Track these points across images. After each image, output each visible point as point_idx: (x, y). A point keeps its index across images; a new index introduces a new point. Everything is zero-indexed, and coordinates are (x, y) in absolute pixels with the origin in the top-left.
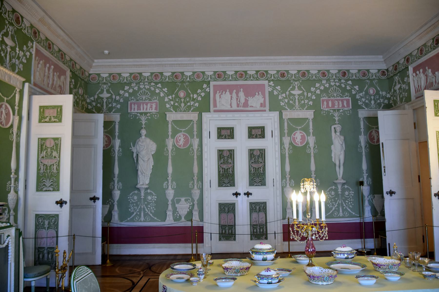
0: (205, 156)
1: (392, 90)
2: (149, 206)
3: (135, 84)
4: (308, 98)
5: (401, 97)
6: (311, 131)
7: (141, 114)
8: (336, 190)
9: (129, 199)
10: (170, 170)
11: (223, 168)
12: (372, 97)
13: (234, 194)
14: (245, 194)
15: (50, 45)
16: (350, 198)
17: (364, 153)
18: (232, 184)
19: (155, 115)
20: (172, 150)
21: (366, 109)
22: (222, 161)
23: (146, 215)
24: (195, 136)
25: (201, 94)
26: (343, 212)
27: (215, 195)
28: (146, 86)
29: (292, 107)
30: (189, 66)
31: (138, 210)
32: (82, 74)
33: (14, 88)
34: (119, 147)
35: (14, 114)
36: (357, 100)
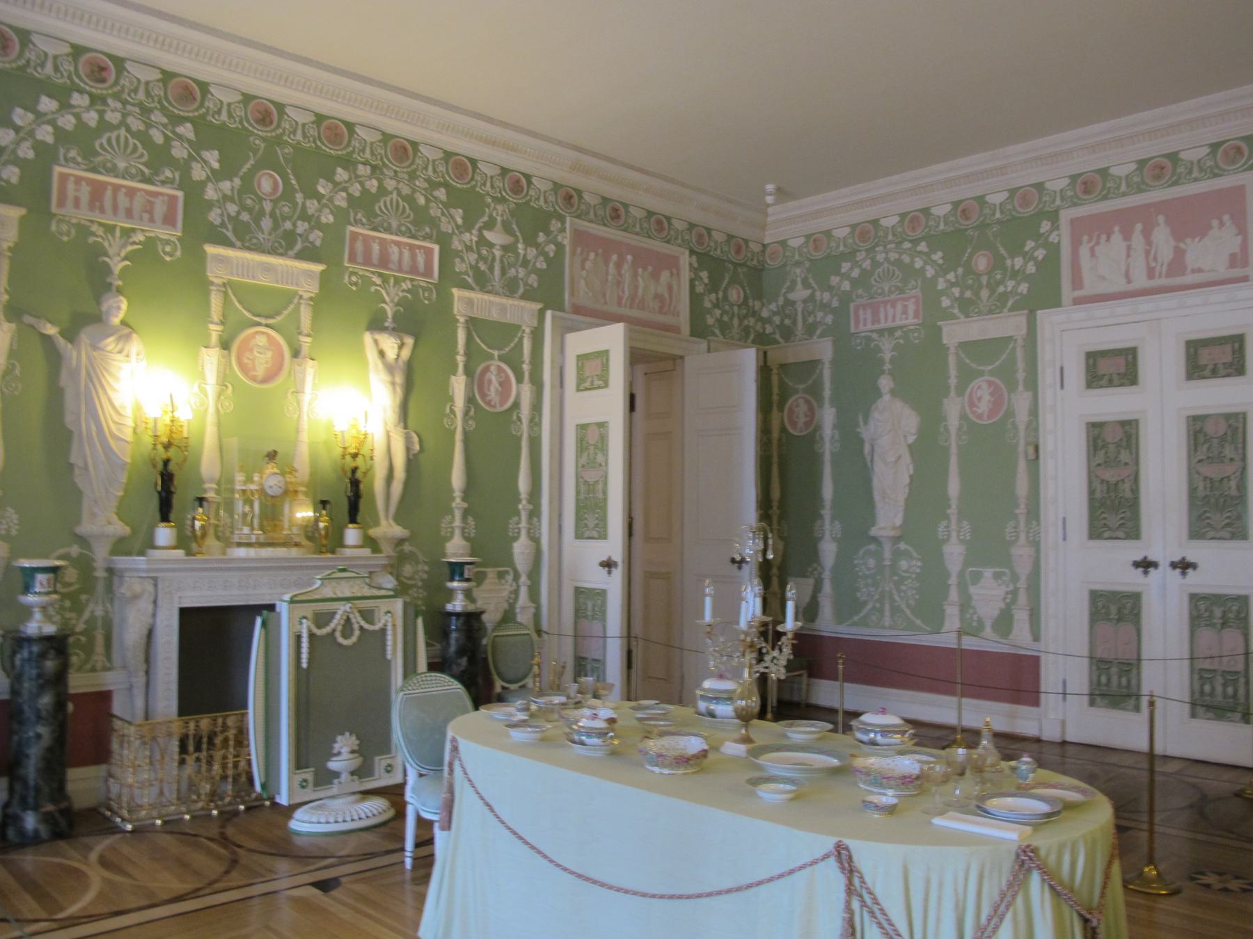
0: (1048, 444)
2: (903, 588)
7: (880, 332)
10: (954, 487)
11: (1102, 481)
13: (1137, 564)
14: (1174, 565)
15: (616, 210)
18: (1130, 529)
20: (960, 429)
22: (1100, 457)
24: (1021, 383)
25: (1036, 254)
27: (1076, 566)
30: (992, 175)
32: (738, 252)
33: (519, 327)
34: (835, 427)
35: (520, 380)
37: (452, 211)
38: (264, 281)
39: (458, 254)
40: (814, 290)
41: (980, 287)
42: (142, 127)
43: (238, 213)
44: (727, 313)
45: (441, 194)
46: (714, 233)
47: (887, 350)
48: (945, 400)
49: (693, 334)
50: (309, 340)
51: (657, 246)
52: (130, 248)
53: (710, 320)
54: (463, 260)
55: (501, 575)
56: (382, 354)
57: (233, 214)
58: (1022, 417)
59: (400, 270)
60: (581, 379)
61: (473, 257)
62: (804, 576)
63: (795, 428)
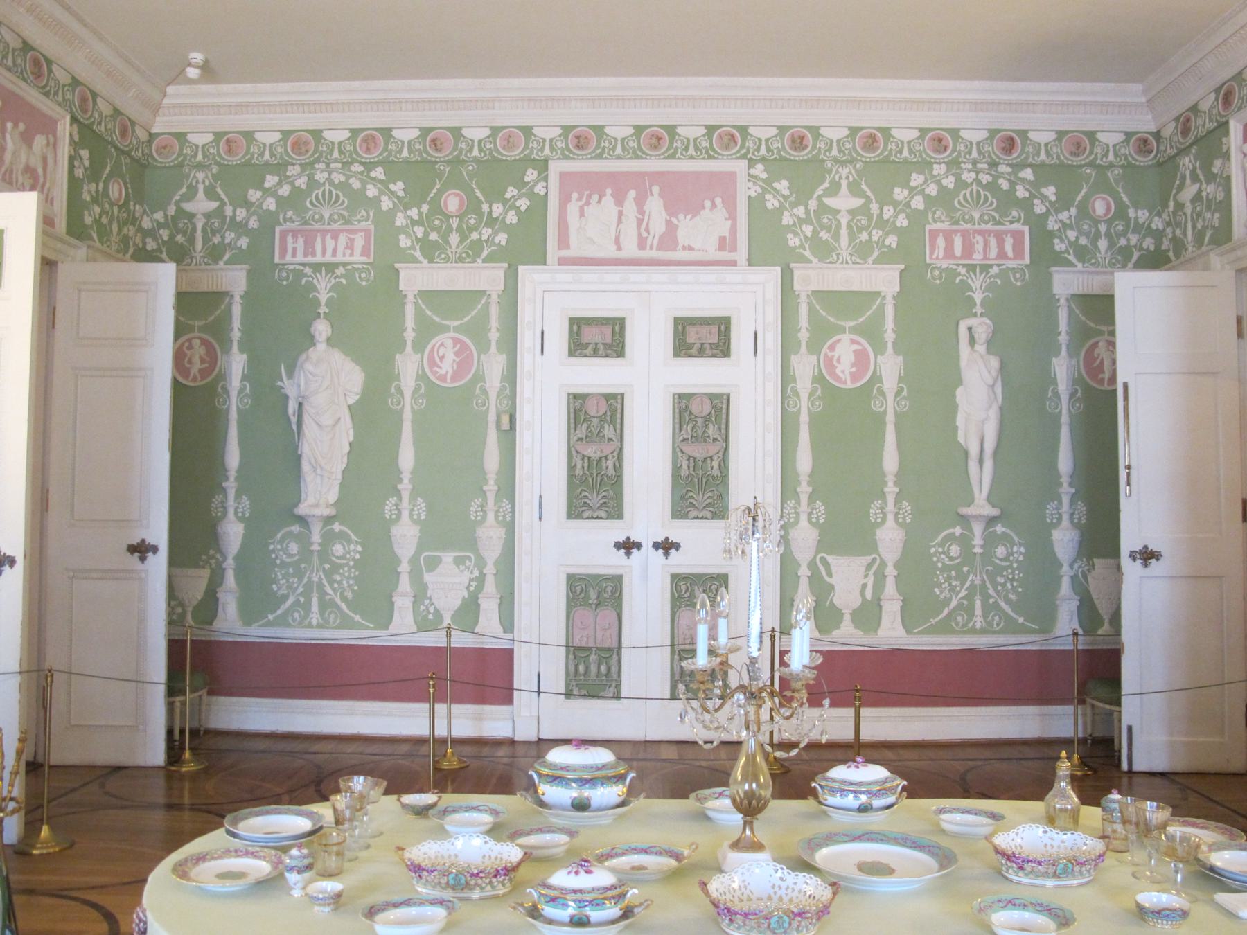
0: (524, 414)
1: (1172, 204)
2: (338, 577)
3: (298, 169)
4: (882, 223)
5: (1199, 226)
6: (890, 336)
7: (317, 267)
8: (965, 541)
9: (273, 551)
10: (407, 458)
11: (584, 456)
12: (1103, 228)
13: (618, 546)
14: (656, 546)
16: (1011, 567)
17: (1065, 418)
18: (614, 509)
19: (360, 271)
21: (1080, 265)
22: (582, 431)
25: (518, 203)
26: (985, 615)
27: (556, 546)
28: (334, 175)
29: (824, 251)
30: (478, 105)
31: (301, 589)
32: (123, 134)
34: (244, 378)
36: (1051, 234)
40: (223, 204)
41: (450, 229)
47: (324, 289)
48: (398, 356)
49: (69, 233)
51: (32, 95)
53: (88, 220)
58: (494, 381)
62: (197, 566)
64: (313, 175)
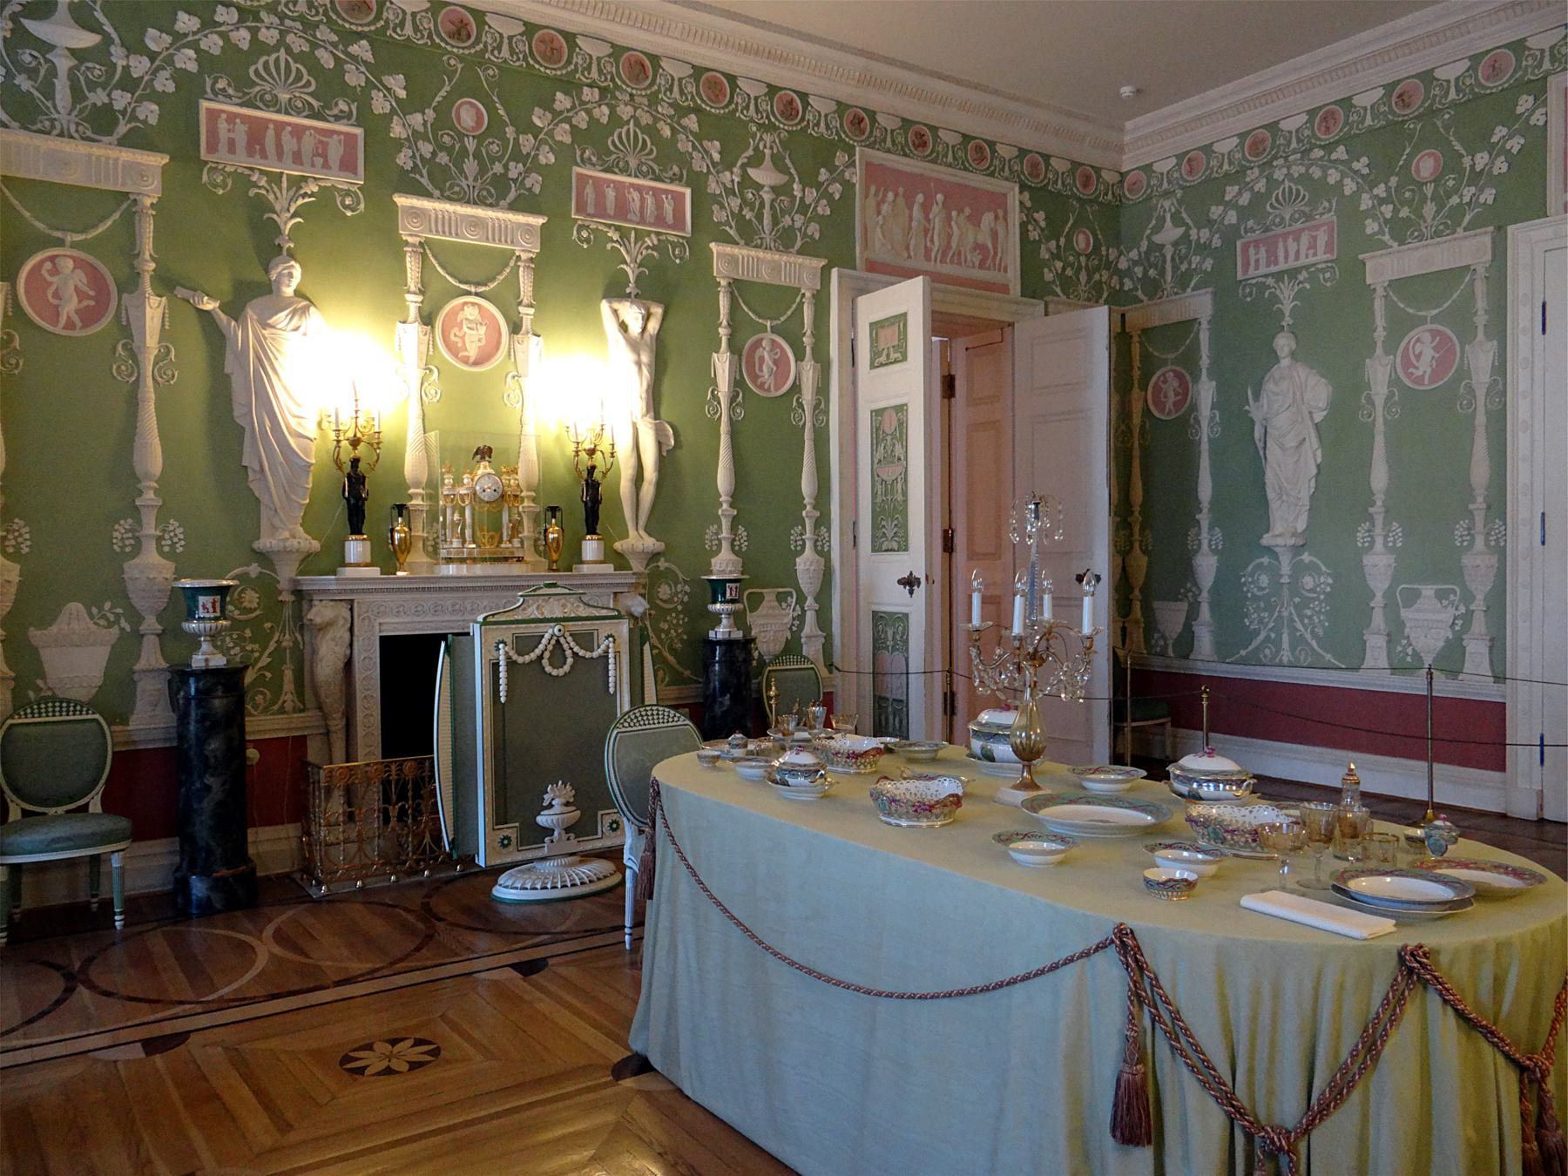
2: (1309, 612)
3: (1256, 171)
7: (1278, 276)
10: (1379, 477)
19: (1323, 271)
23: (1297, 641)
35: (800, 357)
37: (705, 143)
38: (470, 239)
39: (716, 199)
40: (1188, 228)
41: (1424, 200)
42: (306, 48)
43: (434, 154)
44: (1072, 265)
45: (692, 122)
46: (1053, 161)
48: (1368, 361)
50: (532, 311)
51: (977, 180)
52: (300, 201)
53: (1048, 276)
54: (722, 207)
55: (781, 598)
56: (623, 327)
57: (428, 156)
58: (1482, 377)
59: (642, 221)
60: (875, 354)
61: (735, 203)
62: (1177, 600)
63: (1162, 410)
64: (1271, 174)
